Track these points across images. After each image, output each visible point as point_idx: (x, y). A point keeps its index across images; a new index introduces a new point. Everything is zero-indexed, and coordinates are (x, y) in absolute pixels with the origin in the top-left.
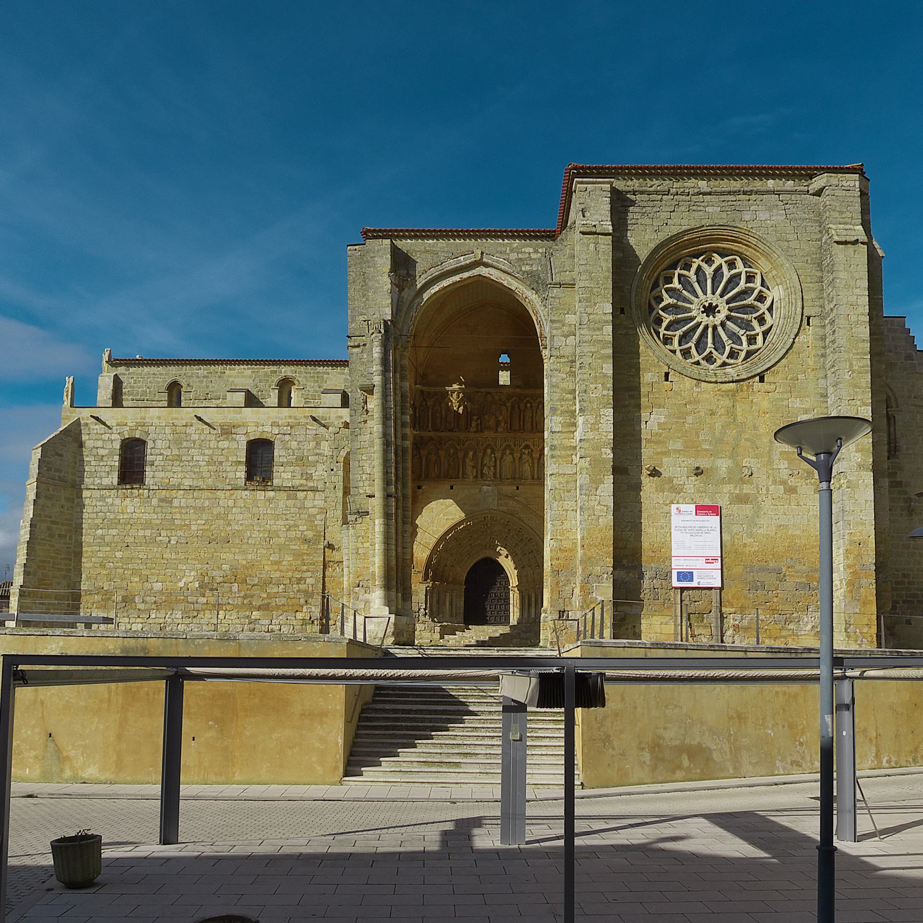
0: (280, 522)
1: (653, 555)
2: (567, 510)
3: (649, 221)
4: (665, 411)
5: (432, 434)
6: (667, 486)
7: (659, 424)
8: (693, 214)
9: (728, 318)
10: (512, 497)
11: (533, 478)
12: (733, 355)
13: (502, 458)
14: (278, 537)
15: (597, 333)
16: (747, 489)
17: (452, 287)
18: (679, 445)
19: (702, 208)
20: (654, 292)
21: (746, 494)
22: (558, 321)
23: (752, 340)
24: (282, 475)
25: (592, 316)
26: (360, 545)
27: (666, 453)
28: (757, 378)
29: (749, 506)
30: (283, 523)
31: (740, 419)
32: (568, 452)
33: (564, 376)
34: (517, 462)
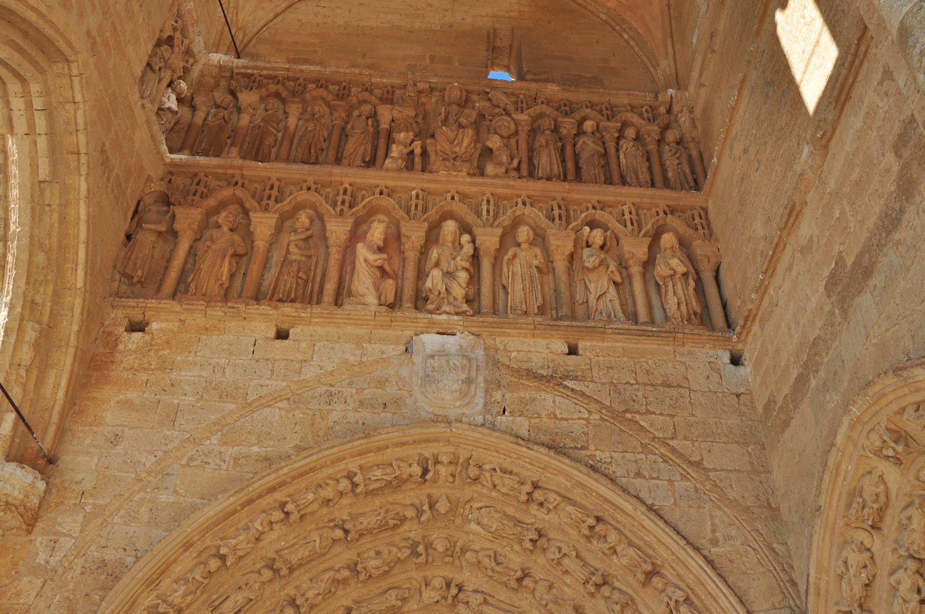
11: (633, 317)
34: (560, 265)
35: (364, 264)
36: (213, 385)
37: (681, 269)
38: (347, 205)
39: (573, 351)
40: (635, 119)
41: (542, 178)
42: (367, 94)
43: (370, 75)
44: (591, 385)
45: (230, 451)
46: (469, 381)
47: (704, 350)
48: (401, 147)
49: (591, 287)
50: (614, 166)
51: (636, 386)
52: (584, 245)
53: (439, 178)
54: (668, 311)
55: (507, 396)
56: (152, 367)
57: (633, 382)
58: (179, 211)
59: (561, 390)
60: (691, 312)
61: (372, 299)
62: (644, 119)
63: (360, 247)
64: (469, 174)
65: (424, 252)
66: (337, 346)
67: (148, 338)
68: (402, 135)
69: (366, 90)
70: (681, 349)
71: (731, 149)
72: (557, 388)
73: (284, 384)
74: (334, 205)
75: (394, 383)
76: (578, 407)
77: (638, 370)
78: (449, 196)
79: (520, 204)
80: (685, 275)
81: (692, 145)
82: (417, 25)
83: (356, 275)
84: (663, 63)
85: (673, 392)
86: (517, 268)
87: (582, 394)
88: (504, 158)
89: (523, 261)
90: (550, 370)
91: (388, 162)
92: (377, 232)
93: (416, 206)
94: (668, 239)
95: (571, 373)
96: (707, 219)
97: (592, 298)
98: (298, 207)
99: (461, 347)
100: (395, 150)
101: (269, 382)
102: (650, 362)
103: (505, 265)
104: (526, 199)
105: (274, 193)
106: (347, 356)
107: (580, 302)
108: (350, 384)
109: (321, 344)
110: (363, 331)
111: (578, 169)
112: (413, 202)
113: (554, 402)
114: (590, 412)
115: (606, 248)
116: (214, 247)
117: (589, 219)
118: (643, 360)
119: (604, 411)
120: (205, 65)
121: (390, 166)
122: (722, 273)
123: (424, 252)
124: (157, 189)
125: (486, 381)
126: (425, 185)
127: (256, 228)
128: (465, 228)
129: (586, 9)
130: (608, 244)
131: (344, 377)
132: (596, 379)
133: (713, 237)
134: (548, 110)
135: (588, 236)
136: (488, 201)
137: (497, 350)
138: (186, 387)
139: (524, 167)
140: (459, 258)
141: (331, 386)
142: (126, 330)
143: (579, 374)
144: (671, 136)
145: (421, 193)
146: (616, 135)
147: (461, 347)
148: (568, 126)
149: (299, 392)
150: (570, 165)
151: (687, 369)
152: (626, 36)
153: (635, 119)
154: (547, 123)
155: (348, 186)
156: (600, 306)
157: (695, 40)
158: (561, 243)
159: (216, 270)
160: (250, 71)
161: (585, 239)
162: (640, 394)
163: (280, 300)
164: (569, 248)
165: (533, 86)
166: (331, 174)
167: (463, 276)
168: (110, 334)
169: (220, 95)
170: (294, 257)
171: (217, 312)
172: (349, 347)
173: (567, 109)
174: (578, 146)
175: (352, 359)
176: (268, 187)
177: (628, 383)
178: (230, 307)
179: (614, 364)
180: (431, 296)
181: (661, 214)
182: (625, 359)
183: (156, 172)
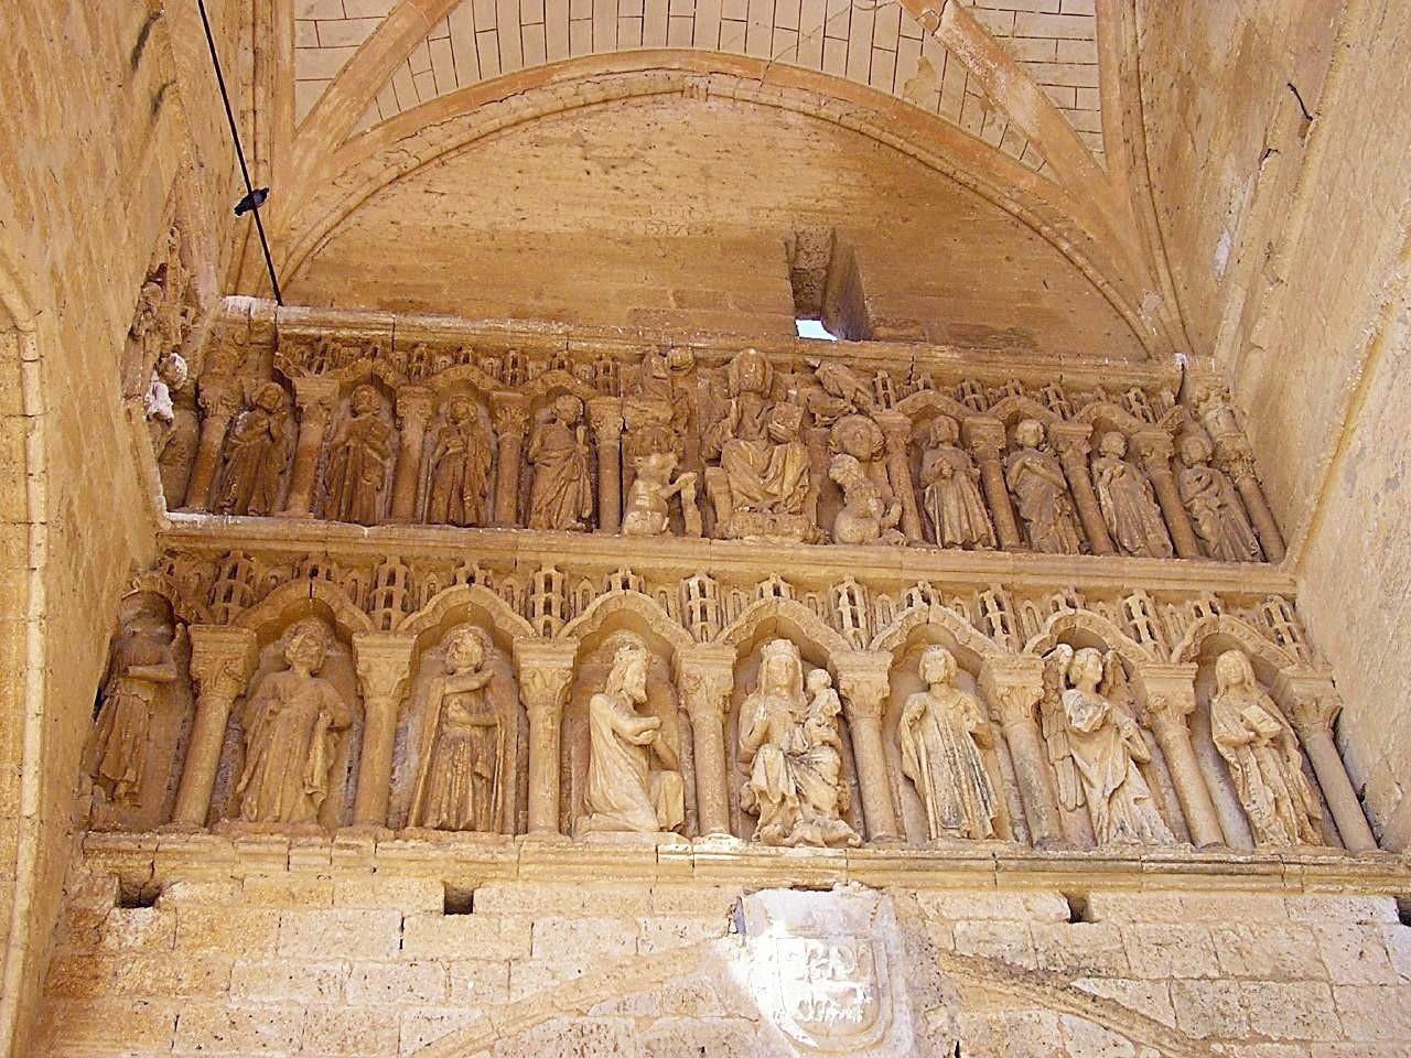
10: (1046, 977)
13: (888, 714)
34: (1021, 730)
35: (613, 742)
36: (323, 1021)
37: (1270, 727)
38: (556, 612)
39: (1078, 915)
40: (1118, 417)
41: (952, 544)
42: (563, 373)
43: (567, 334)
44: (1131, 986)
47: (1345, 898)
48: (656, 486)
49: (1092, 772)
50: (1090, 514)
51: (1221, 984)
52: (1062, 684)
53: (744, 551)
54: (1255, 817)
55: (959, 1019)
56: (184, 985)
57: (1214, 973)
59: (1072, 999)
60: (1303, 817)
61: (643, 818)
62: (1133, 414)
63: (598, 702)
64: (805, 540)
65: (731, 712)
66: (583, 924)
67: (167, 919)
68: (654, 460)
69: (561, 366)
70: (1299, 899)
71: (1351, 478)
72: (1060, 995)
73: (478, 1013)
74: (529, 614)
75: (715, 1002)
76: (1111, 1035)
77: (1221, 948)
78: (768, 587)
79: (918, 600)
80: (1277, 742)
81: (1238, 467)
82: (639, 230)
83: (596, 767)
84: (1150, 300)
85: (1299, 991)
86: (932, 736)
87: (1116, 1006)
88: (874, 505)
89: (944, 719)
90: (1041, 957)
91: (631, 518)
92: (631, 668)
93: (703, 611)
94: (1230, 665)
95: (1083, 963)
96: (1298, 621)
97: (1096, 798)
98: (455, 619)
99: (847, 914)
100: (645, 493)
101: (444, 1011)
102: (1240, 928)
103: (905, 732)
104: (928, 589)
105: (398, 590)
106: (605, 947)
107: (1071, 805)
108: (622, 1007)
109: (549, 920)
110: (633, 891)
111: (1021, 522)
112: (696, 602)
113: (1060, 1025)
114: (1136, 1044)
115: (1105, 689)
116: (284, 712)
117: (1062, 628)
118: (1225, 925)
119: (1166, 1041)
120: (218, 319)
121: (638, 526)
122: (1346, 732)
123: (731, 712)
124: (145, 587)
125: (911, 988)
126: (716, 567)
127: (369, 669)
128: (812, 658)
129: (974, 190)
130: (1110, 679)
131: (604, 993)
132: (1139, 973)
133: (1319, 658)
134: (941, 401)
135: (1070, 665)
136: (852, 598)
137: (922, 916)
138: (263, 1029)
139: (912, 521)
140: (812, 722)
141: (581, 1013)
142: (116, 905)
143: (1102, 962)
144: (1195, 448)
145: (708, 582)
146: (1086, 449)
147: (847, 914)
148: (986, 429)
149: (513, 1030)
150: (1004, 515)
151: (1316, 940)
152: (1065, 246)
153: (1118, 417)
154: (943, 427)
155: (553, 572)
156: (1118, 813)
157: (1222, 255)
158: (1016, 679)
159: (290, 760)
160: (312, 331)
161: (1062, 670)
162: (1233, 999)
164: (1036, 691)
165: (905, 351)
166: (515, 547)
167: (828, 760)
168: (84, 913)
169: (256, 384)
170: (458, 731)
171: (312, 856)
172: (606, 926)
173: (982, 396)
174: (1013, 473)
175: (617, 950)
176: (384, 578)
177: (1204, 977)
178: (340, 846)
179: (1169, 939)
180: (765, 807)
181: (1207, 612)
182: (1191, 926)
183: (141, 551)
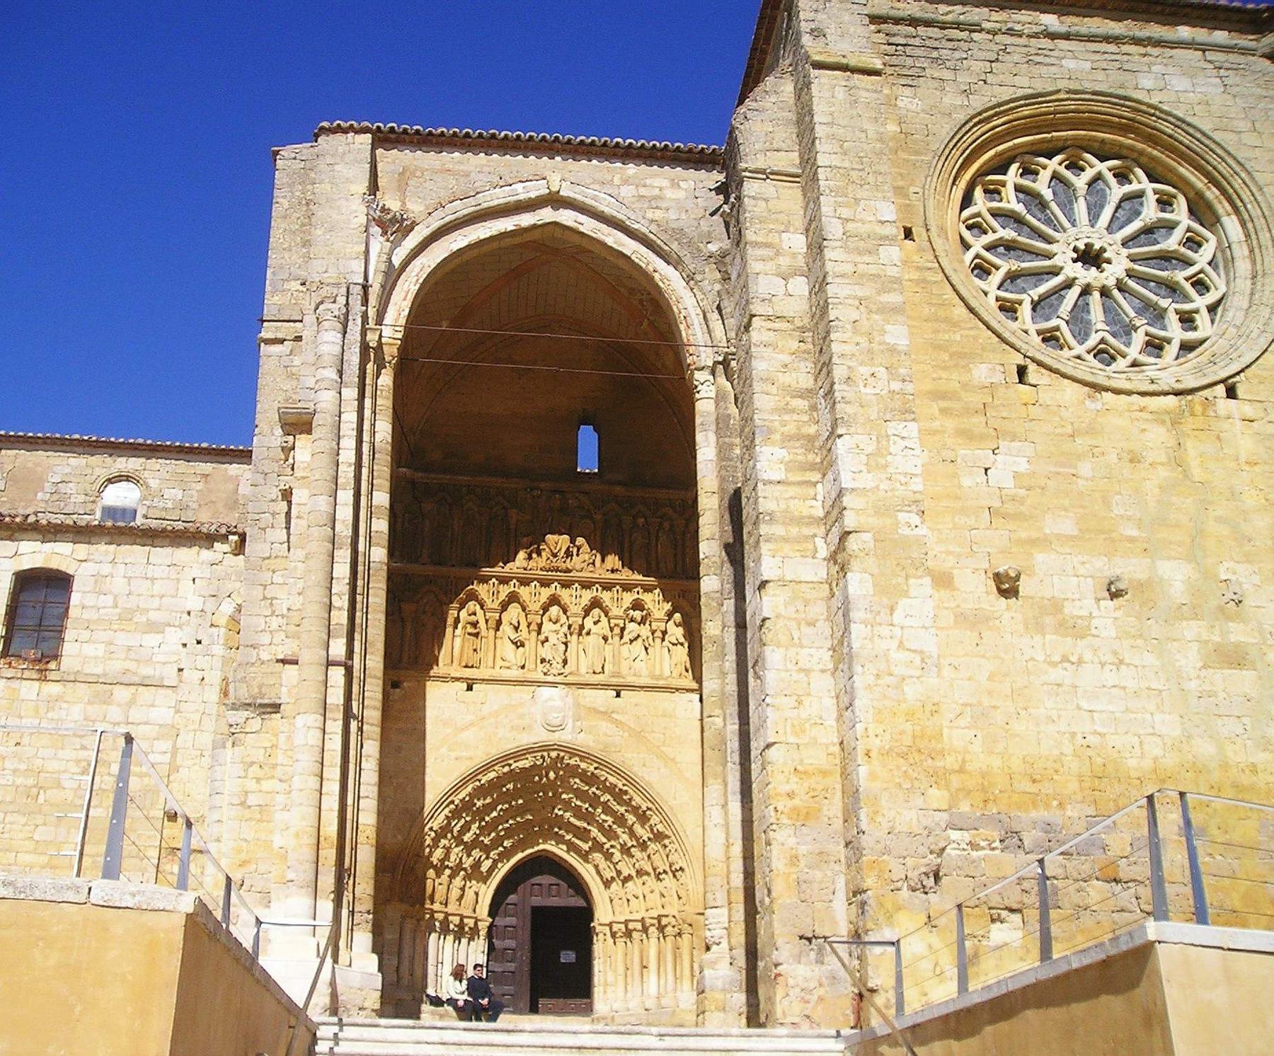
0: (68, 753)
1: (1033, 789)
2: (807, 671)
3: (947, 75)
4: (1028, 449)
5: (429, 570)
6: (1048, 620)
7: (1016, 476)
8: (1036, 70)
9: (1130, 274)
10: (606, 714)
12: (1155, 346)
14: (59, 786)
15: (867, 259)
16: (1238, 633)
17: (495, 245)
18: (1067, 526)
19: (1052, 60)
20: (966, 213)
21: (1238, 645)
22: (767, 245)
23: (1187, 320)
24: (79, 647)
25: (850, 226)
26: (252, 785)
27: (1042, 542)
28: (1221, 389)
29: (1248, 675)
30: (74, 755)
31: (1197, 473)
32: (807, 531)
33: (786, 358)
45: (453, 754)
46: (564, 717)
58: (404, 606)
163: (466, 666)
